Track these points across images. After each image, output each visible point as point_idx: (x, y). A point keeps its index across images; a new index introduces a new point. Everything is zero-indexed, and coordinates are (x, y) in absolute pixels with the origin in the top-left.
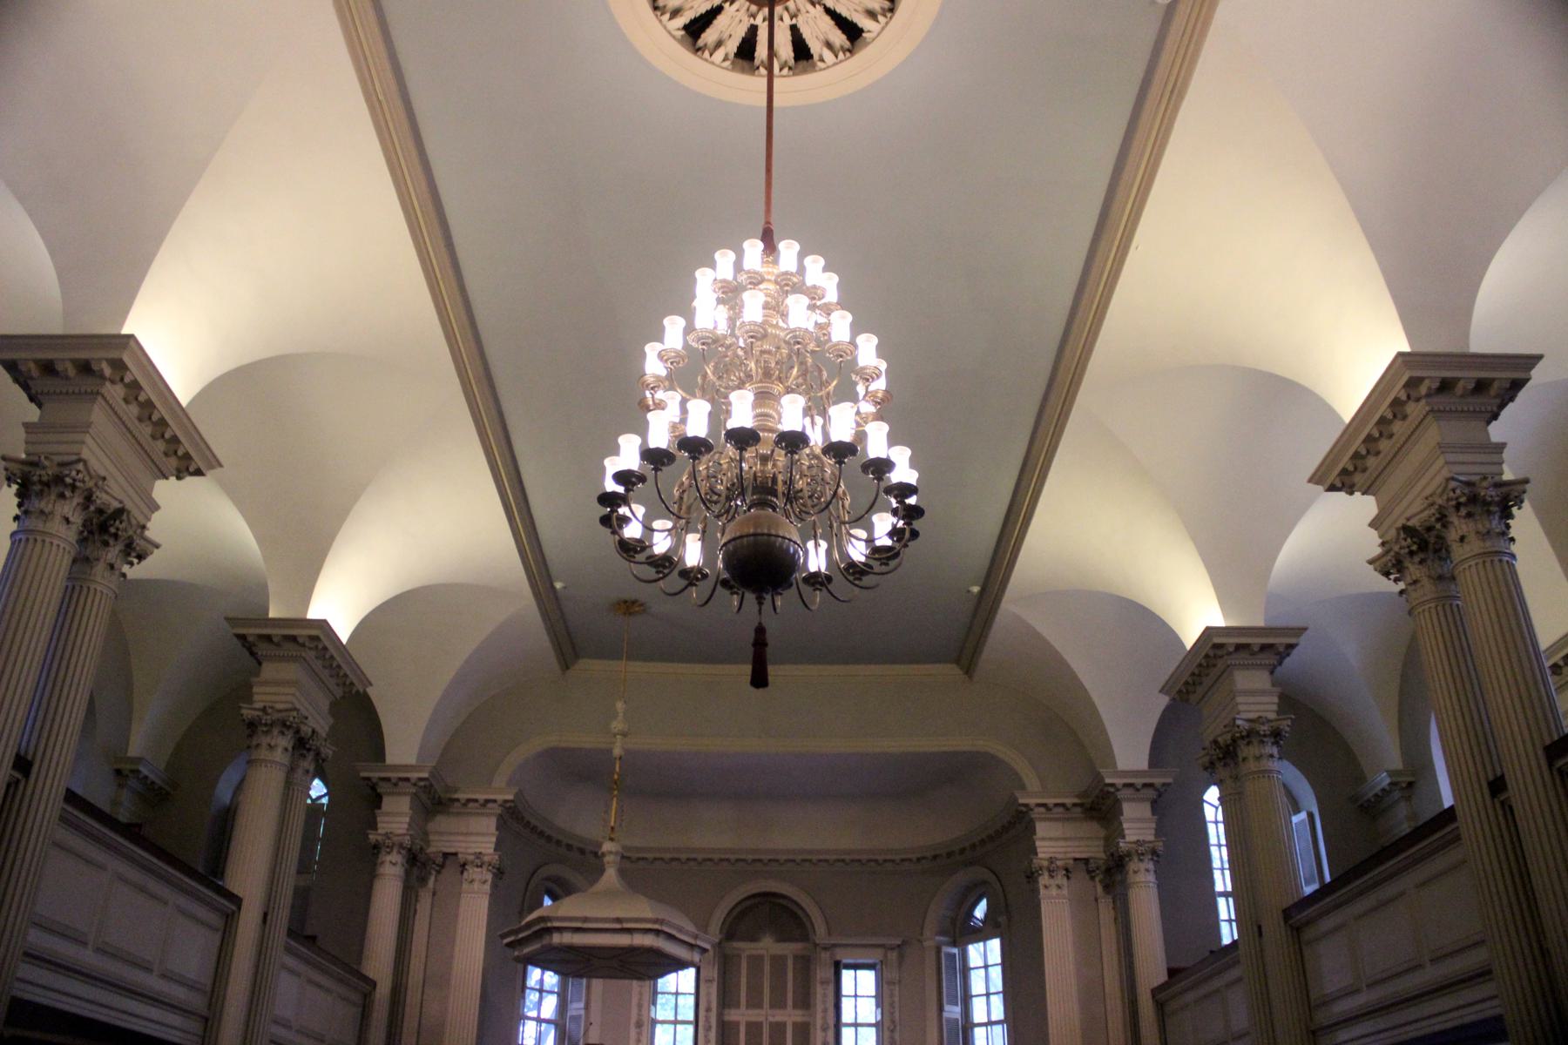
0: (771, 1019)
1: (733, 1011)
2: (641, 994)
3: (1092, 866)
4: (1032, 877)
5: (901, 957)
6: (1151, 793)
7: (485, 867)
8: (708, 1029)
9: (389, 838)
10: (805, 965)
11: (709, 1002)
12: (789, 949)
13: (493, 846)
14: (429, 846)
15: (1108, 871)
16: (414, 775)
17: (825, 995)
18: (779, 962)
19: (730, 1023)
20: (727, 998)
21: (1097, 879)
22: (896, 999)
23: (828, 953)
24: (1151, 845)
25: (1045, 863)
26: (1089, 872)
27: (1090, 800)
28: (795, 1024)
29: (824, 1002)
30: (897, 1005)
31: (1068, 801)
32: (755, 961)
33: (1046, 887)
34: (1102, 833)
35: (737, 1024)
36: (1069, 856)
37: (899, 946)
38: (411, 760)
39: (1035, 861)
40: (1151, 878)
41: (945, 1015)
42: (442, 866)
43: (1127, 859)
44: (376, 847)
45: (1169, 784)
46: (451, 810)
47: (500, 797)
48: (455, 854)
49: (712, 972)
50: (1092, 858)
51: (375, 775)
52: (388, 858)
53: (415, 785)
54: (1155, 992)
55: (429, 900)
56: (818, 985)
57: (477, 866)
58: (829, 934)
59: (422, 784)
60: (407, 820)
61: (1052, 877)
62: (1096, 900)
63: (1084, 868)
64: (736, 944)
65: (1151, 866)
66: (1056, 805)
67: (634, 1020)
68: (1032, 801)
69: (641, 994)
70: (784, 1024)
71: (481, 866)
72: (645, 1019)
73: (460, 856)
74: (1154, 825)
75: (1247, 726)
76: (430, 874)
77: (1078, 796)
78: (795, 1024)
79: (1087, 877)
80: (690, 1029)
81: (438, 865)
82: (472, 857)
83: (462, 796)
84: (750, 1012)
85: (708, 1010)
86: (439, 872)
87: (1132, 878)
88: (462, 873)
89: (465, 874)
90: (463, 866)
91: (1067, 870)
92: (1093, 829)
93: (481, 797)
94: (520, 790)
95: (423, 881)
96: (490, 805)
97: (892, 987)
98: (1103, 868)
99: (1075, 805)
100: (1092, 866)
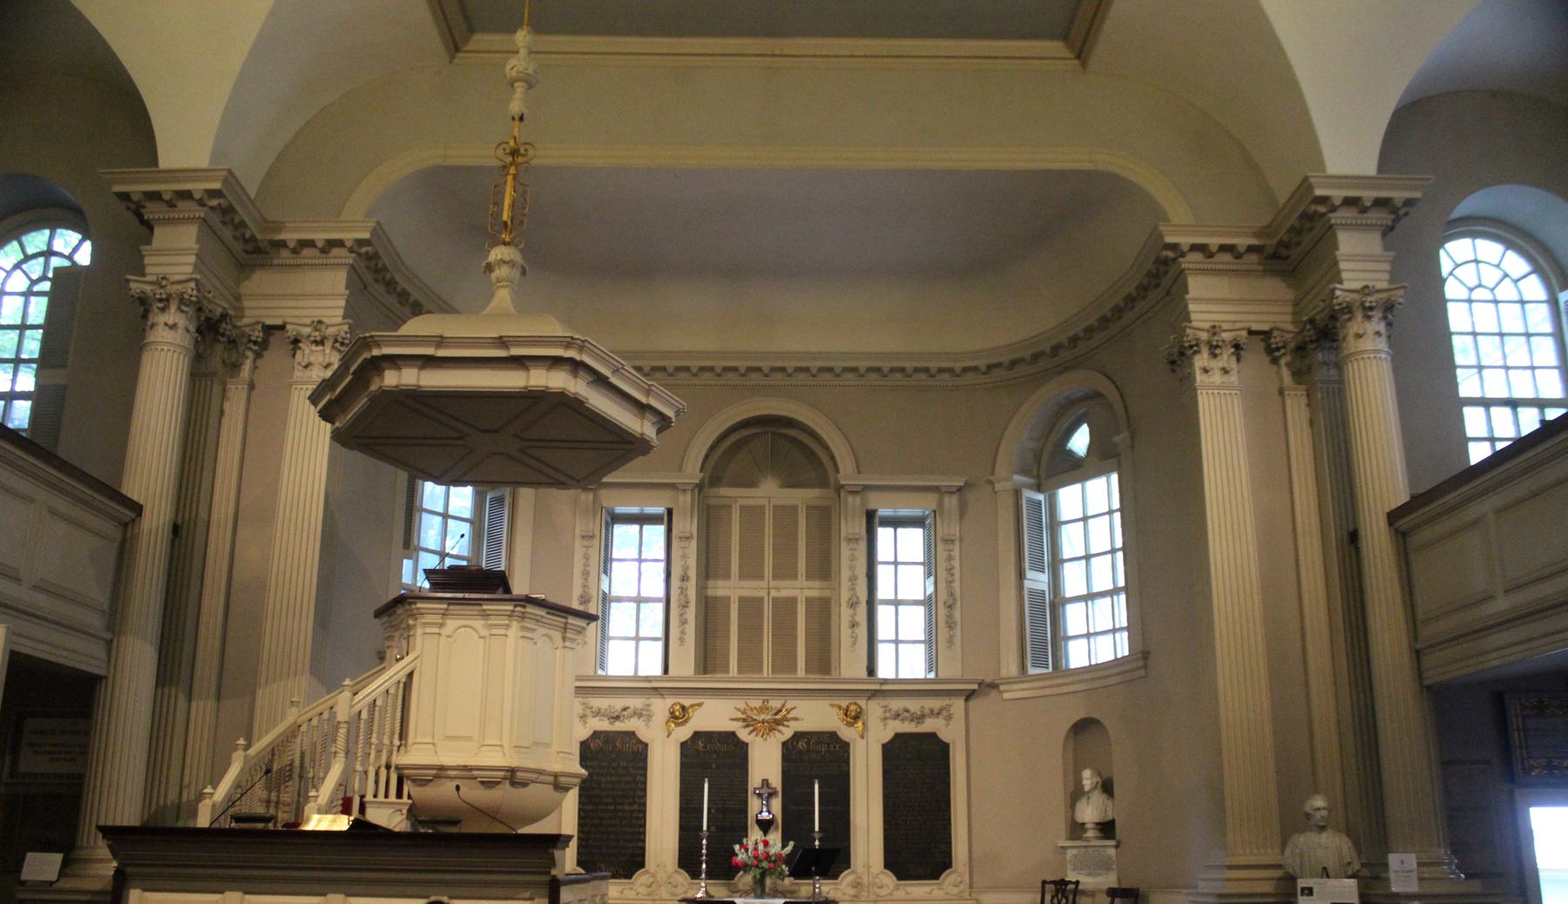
0: (774, 593)
1: (720, 583)
2: (586, 557)
3: (1276, 340)
4: (1179, 359)
5: (963, 509)
6: (1381, 217)
7: (328, 344)
8: (685, 606)
9: (162, 287)
10: (824, 521)
11: (686, 568)
12: (801, 497)
13: (341, 312)
14: (242, 317)
15: (1301, 349)
16: (197, 187)
17: (853, 559)
18: (785, 515)
20: (710, 566)
21: (1283, 361)
22: (956, 563)
23: (858, 499)
24: (1384, 295)
25: (1204, 336)
26: (1269, 350)
27: (1275, 241)
28: (809, 601)
29: (852, 568)
30: (957, 571)
31: (1242, 242)
32: (752, 515)
33: (1206, 371)
34: (1290, 295)
36: (1238, 325)
37: (960, 489)
38: (200, 160)
39: (1188, 331)
40: (1382, 344)
41: (1027, 584)
42: (264, 345)
43: (1346, 317)
44: (144, 302)
46: (276, 262)
47: (348, 236)
48: (282, 327)
49: (687, 525)
50: (1278, 329)
51: (135, 189)
52: (161, 319)
53: (201, 203)
54: (1394, 516)
55: (244, 395)
56: (843, 544)
57: (316, 343)
58: (859, 472)
59: (214, 202)
60: (192, 259)
61: (1215, 356)
62: (1281, 392)
63: (1262, 345)
64: (724, 491)
65: (1382, 327)
66: (1223, 248)
68: (1185, 241)
69: (586, 557)
70: (794, 600)
71: (321, 343)
72: (593, 592)
73: (288, 327)
74: (1387, 267)
76: (247, 358)
77: (1256, 235)
78: (809, 601)
79: (1266, 359)
80: (659, 608)
81: (255, 343)
82: (306, 331)
83: (291, 237)
84: (745, 583)
85: (684, 578)
86: (258, 355)
87: (1351, 345)
88: (294, 356)
89: (299, 353)
90: (296, 341)
91: (1237, 347)
92: (1273, 287)
93: (320, 237)
94: (378, 223)
95: (235, 367)
96: (335, 251)
97: (951, 547)
98: (1292, 345)
99: (1251, 249)
100: (1276, 340)
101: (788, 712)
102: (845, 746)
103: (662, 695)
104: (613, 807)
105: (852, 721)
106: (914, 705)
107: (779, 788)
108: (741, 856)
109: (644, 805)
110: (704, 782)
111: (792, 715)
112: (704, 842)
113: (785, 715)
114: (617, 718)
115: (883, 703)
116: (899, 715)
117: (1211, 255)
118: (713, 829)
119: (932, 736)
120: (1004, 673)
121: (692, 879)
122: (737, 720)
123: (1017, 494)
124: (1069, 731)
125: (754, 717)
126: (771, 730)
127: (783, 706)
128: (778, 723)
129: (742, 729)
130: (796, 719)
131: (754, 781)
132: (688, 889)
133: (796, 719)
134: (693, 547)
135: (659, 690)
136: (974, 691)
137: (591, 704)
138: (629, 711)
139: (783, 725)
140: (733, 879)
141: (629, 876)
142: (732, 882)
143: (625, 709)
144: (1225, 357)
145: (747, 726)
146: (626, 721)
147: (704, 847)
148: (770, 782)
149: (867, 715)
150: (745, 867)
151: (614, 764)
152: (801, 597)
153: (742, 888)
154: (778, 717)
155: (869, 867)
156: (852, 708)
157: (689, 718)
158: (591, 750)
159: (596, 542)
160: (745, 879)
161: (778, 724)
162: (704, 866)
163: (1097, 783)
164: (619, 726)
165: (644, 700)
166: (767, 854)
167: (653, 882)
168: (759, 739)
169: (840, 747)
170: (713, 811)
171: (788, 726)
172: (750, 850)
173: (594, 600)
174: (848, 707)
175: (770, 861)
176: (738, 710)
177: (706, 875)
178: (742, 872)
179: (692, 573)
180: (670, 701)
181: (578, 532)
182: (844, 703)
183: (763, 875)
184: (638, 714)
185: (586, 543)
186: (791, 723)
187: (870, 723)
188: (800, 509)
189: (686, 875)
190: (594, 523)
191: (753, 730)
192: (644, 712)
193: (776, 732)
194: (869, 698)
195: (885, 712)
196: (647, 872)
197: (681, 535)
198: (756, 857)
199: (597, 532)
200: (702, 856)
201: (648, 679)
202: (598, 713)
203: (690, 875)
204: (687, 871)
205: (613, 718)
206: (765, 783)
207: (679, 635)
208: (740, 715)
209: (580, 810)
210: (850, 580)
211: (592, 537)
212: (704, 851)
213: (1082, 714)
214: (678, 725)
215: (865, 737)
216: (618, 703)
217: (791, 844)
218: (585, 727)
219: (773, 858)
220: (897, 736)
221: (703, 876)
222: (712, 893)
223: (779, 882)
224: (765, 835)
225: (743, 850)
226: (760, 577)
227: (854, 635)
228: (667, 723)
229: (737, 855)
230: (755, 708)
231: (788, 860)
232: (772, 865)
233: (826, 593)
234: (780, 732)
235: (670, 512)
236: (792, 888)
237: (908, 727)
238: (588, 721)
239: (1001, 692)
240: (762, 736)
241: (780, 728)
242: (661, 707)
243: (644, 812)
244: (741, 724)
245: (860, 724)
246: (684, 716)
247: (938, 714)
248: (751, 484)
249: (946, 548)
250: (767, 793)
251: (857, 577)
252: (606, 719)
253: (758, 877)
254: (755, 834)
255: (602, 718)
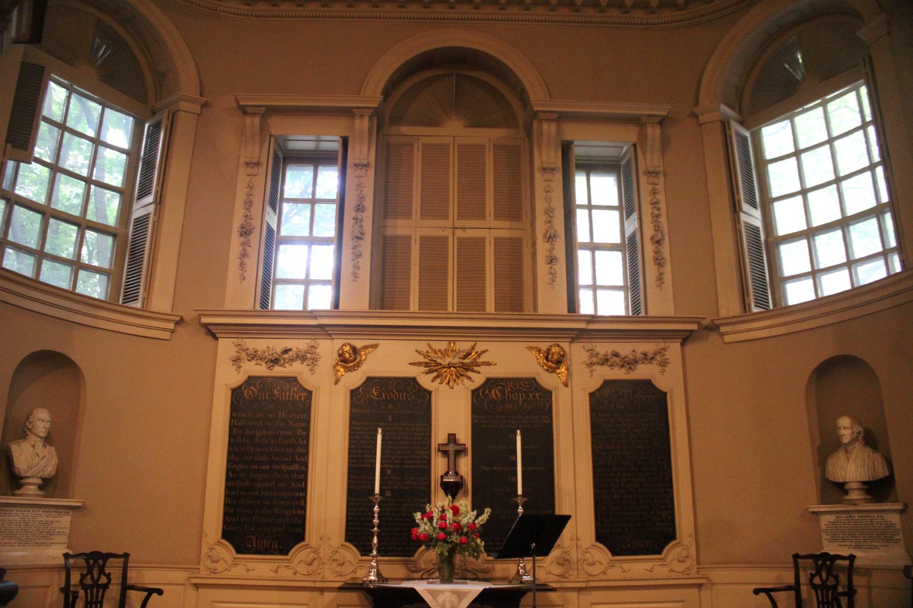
0: (459, 233)
1: (400, 222)
2: (251, 187)
5: (665, 143)
19: (395, 238)
22: (661, 197)
23: (553, 127)
29: (548, 200)
30: (663, 206)
35: (408, 238)
49: (362, 152)
56: (538, 177)
64: (404, 129)
67: (237, 222)
70: (483, 239)
72: (256, 223)
85: (360, 208)
97: (654, 180)
101: (479, 355)
102: (547, 395)
103: (330, 335)
104: (268, 467)
105: (554, 365)
106: (625, 348)
107: (469, 446)
108: (424, 528)
109: (306, 464)
110: (377, 431)
111: (483, 359)
112: (376, 508)
113: (475, 359)
114: (276, 361)
115: (589, 346)
116: (607, 360)
118: (388, 494)
119: (647, 384)
120: (723, 313)
121: (362, 555)
122: (419, 364)
123: (725, 125)
124: (810, 378)
125: (439, 361)
126: (459, 376)
127: (473, 348)
128: (467, 368)
129: (424, 375)
130: (488, 364)
131: (439, 436)
132: (356, 568)
133: (488, 364)
134: (369, 178)
135: (327, 328)
136: (692, 331)
137: (247, 346)
138: (291, 353)
139: (473, 371)
140: (413, 556)
141: (285, 551)
142: (412, 559)
143: (286, 351)
145: (430, 372)
146: (287, 365)
147: (376, 515)
148: (457, 437)
149: (570, 360)
150: (429, 541)
151: (271, 416)
152: (490, 237)
153: (423, 566)
154: (467, 361)
155: (578, 539)
156: (553, 350)
157: (360, 362)
158: (245, 398)
159: (262, 171)
160: (428, 556)
161: (467, 370)
162: (375, 540)
163: (859, 433)
164: (278, 371)
165: (308, 341)
166: (458, 523)
167: (315, 559)
168: (444, 386)
169: (540, 396)
170: (389, 472)
171: (479, 373)
172: (435, 521)
173: (257, 231)
174: (549, 350)
175: (461, 534)
176: (419, 352)
177: (379, 551)
178: (423, 547)
179: (369, 204)
180: (338, 343)
181: (242, 160)
182: (544, 346)
183: (452, 552)
184: (302, 357)
185: (250, 171)
186: (482, 369)
187: (574, 370)
188: (487, 148)
189: (355, 549)
190: (261, 149)
191: (437, 377)
192: (309, 355)
193: (465, 379)
194: (573, 340)
195: (591, 356)
196: (307, 546)
197: (357, 162)
198: (443, 528)
199: (264, 160)
200: (373, 527)
201: (314, 314)
202: (254, 356)
203: (359, 551)
204: (356, 546)
205: (272, 361)
206: (452, 438)
207: (351, 269)
208: (422, 359)
209: (228, 470)
210: (546, 213)
211: (258, 164)
212: (376, 521)
213: (831, 353)
214: (348, 370)
215: (569, 384)
216: (278, 345)
217: (488, 511)
218: (239, 373)
219: (465, 530)
220: (607, 383)
221: (375, 552)
222: (385, 575)
223: (471, 559)
224: (454, 497)
225: (425, 519)
226: (445, 216)
227: (553, 271)
228: (334, 367)
229: (418, 525)
230: (440, 350)
231: (486, 531)
232: (464, 538)
233: (516, 234)
234: (469, 378)
235: (345, 142)
236: (486, 566)
237: (618, 374)
238: (242, 364)
239: (722, 335)
240: (448, 383)
241: (470, 374)
242: (328, 349)
243: (306, 473)
244: (423, 369)
245: (563, 369)
246: (355, 359)
247: (652, 358)
248: (433, 122)
249: (651, 180)
250: (452, 450)
251: (554, 210)
252: (263, 363)
253: (447, 554)
254: (440, 501)
255: (259, 361)
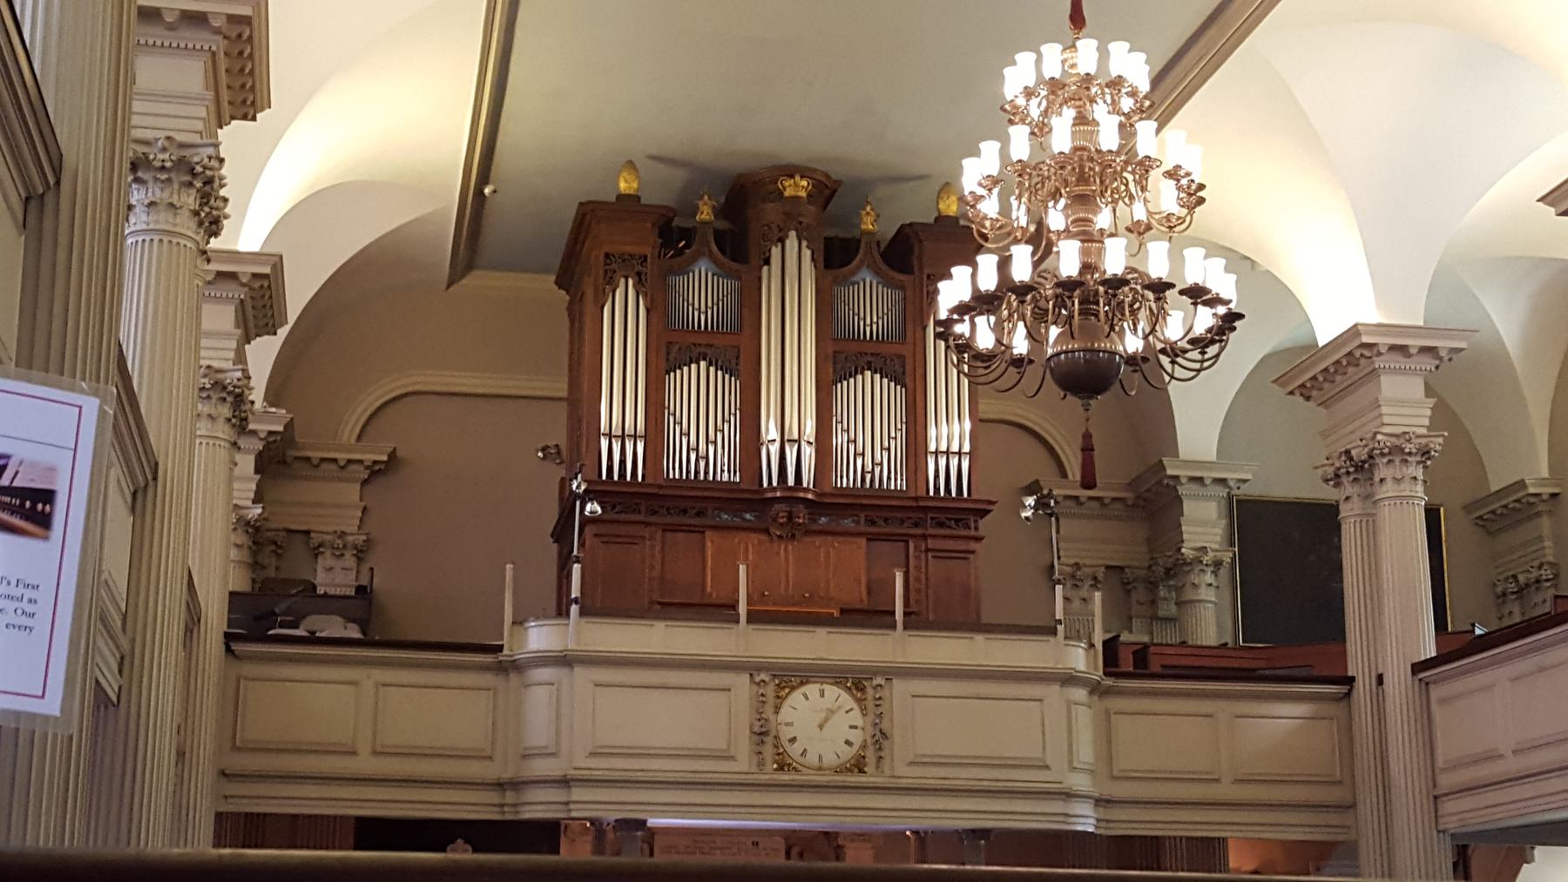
45: (1245, 481)
48: (307, 533)
50: (1128, 567)
75: (1390, 442)
96: (353, 467)
99: (1114, 499)
117: (1082, 504)
144: (1086, 587)
